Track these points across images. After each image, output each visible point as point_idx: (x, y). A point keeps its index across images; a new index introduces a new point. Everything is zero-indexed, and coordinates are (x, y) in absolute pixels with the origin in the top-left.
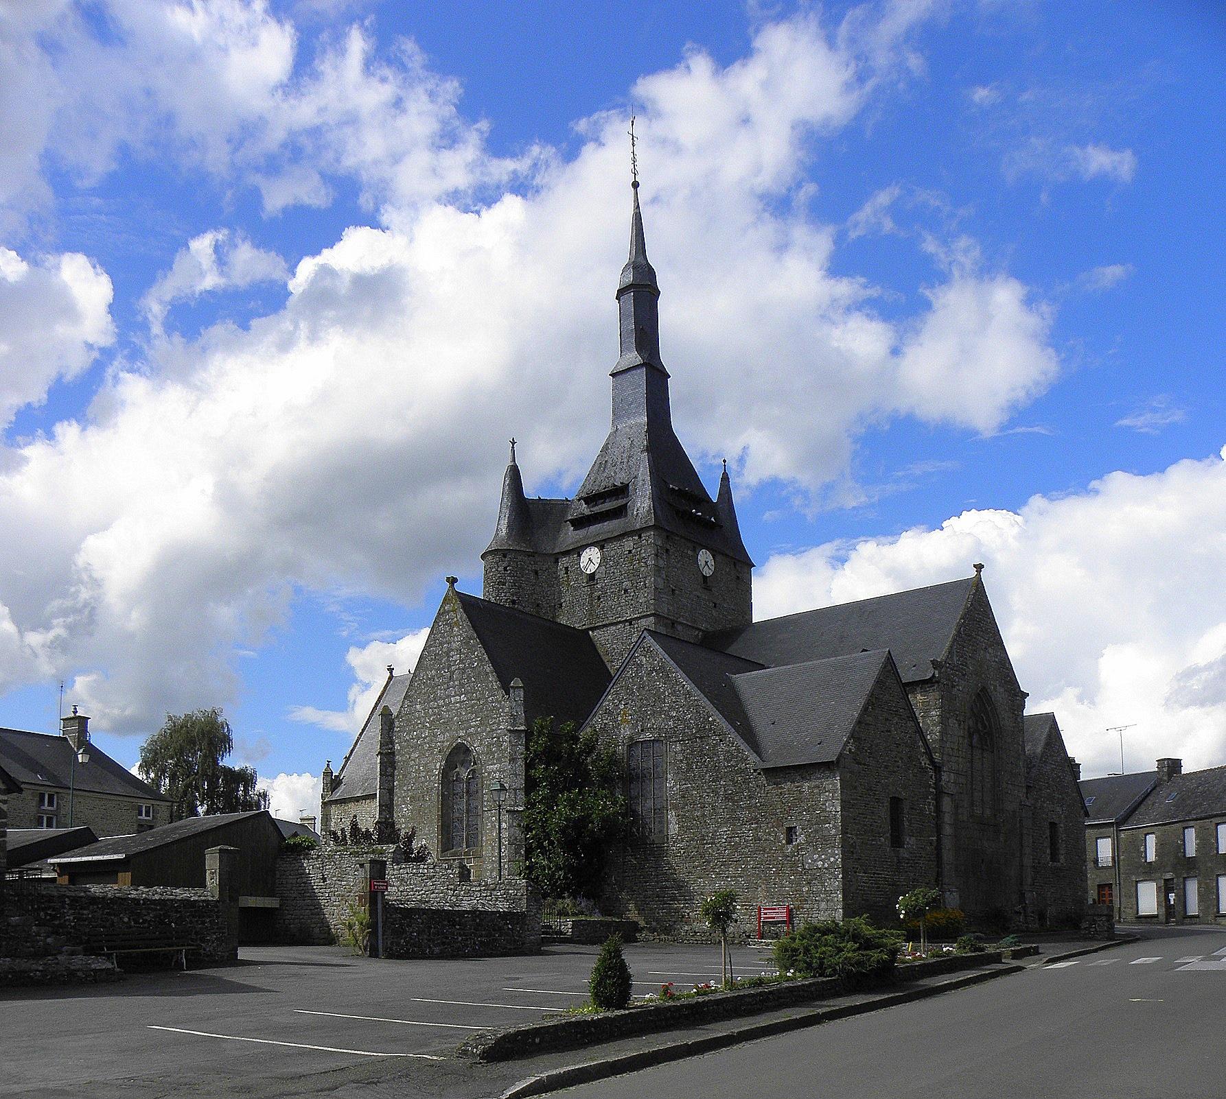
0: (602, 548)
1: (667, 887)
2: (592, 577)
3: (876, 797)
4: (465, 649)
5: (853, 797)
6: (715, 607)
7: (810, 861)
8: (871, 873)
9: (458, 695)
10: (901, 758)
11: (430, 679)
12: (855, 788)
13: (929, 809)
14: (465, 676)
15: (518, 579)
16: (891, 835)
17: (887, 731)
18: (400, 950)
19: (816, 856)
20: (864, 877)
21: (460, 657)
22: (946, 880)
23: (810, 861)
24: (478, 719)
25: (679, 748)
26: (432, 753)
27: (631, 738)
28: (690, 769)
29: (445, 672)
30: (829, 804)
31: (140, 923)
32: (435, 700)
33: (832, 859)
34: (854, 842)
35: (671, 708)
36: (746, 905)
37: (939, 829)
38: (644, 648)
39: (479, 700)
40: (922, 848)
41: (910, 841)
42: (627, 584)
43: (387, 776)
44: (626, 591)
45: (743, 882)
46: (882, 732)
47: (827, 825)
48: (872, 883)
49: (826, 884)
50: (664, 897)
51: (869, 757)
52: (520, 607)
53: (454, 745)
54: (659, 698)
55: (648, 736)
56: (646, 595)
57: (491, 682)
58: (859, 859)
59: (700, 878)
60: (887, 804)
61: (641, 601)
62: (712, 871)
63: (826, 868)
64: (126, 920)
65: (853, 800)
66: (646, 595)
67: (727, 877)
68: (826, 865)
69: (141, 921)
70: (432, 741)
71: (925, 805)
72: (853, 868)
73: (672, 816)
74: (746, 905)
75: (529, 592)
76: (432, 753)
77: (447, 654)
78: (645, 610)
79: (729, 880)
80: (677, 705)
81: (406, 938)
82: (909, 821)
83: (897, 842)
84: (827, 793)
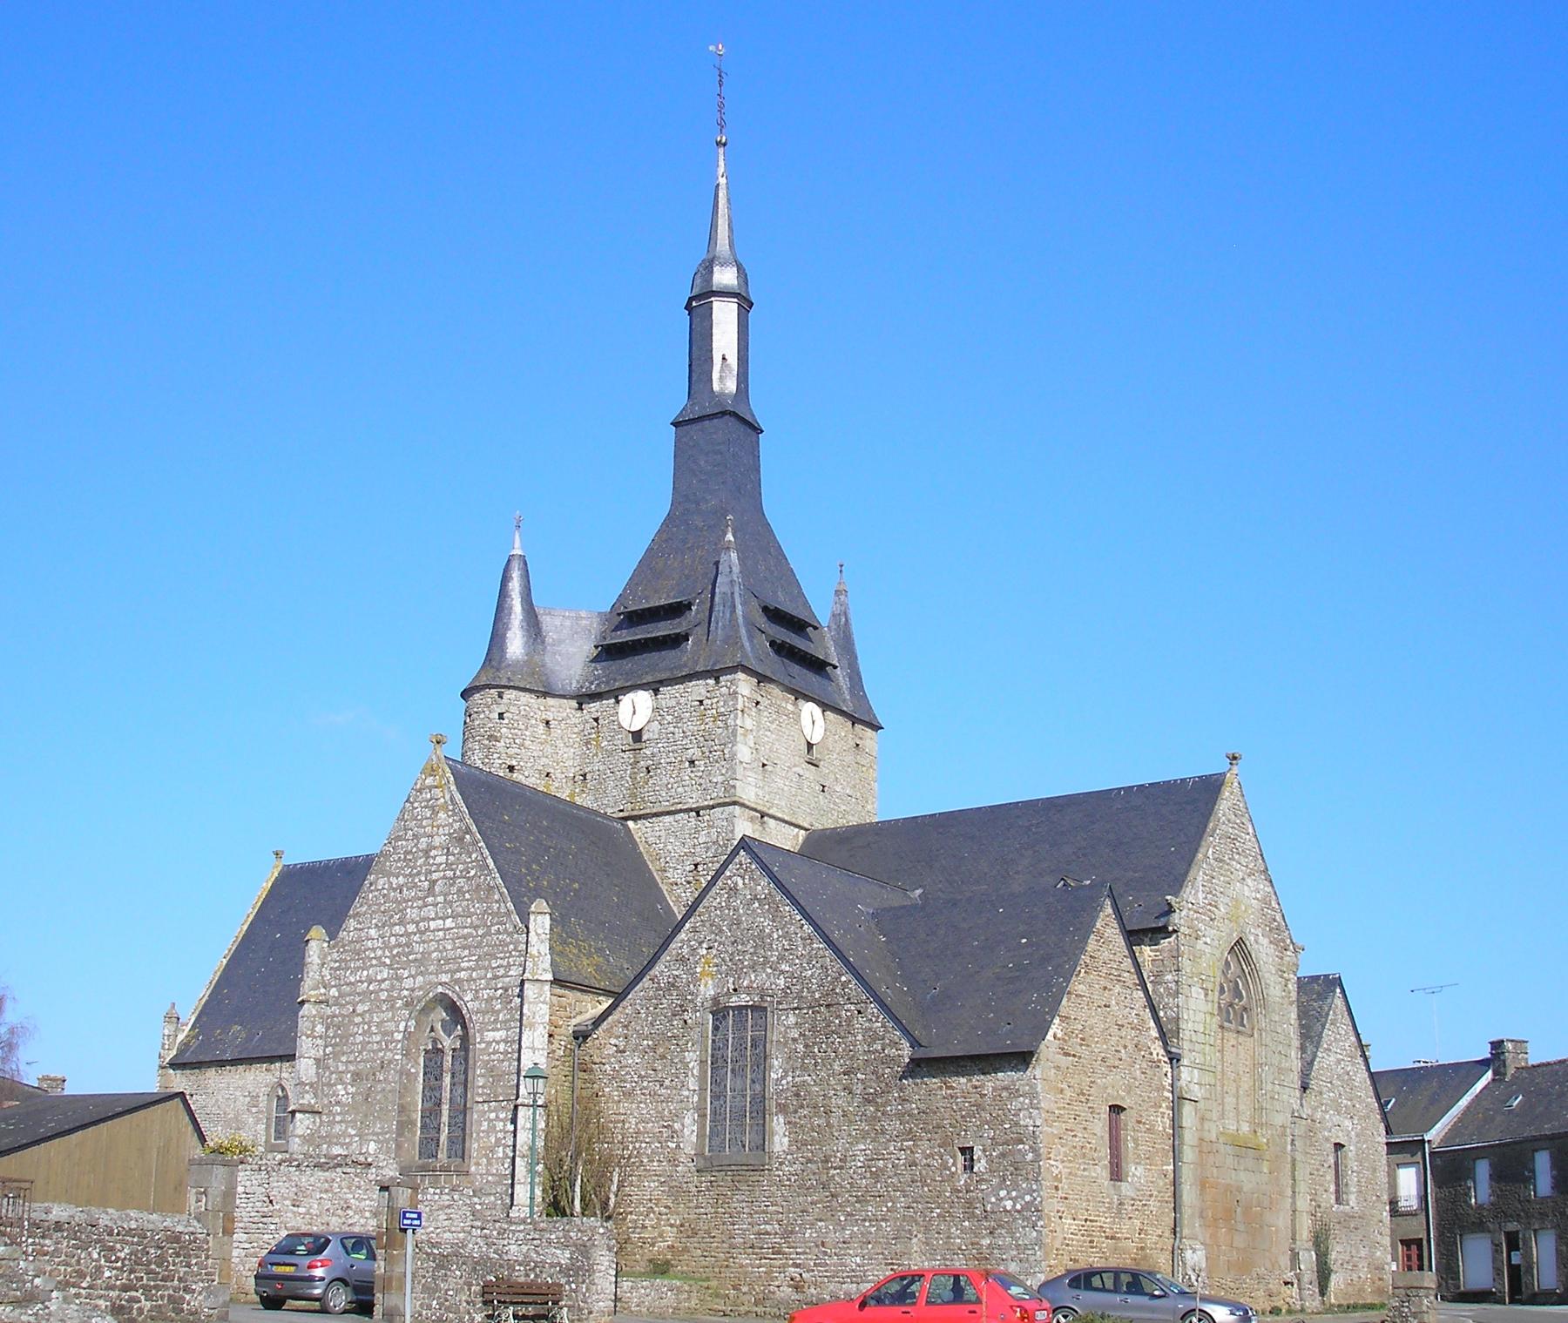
0: (656, 692)
1: (767, 1233)
2: (637, 736)
3: (1089, 1105)
4: (456, 847)
5: (1058, 1105)
6: (823, 791)
7: (993, 1200)
8: (1081, 1220)
9: (441, 918)
10: (1125, 1047)
11: (394, 890)
12: (1062, 1091)
13: (1163, 1123)
14: (454, 890)
15: (519, 733)
16: (1110, 1162)
17: (1105, 1006)
18: (432, 1316)
19: (1003, 1193)
20: (1072, 1225)
21: (447, 859)
22: (1186, 1232)
23: (993, 1200)
24: (474, 958)
25: (792, 1020)
26: (392, 1006)
27: (715, 1000)
28: (808, 1054)
29: (420, 881)
30: (1024, 1116)
31: (111, 1262)
32: (402, 922)
33: (1028, 1198)
34: (1060, 1172)
35: (781, 958)
36: (892, 1264)
37: (1176, 1156)
38: (741, 865)
39: (476, 928)
40: (1152, 1182)
41: (1135, 1172)
42: (694, 752)
43: (316, 1037)
44: (692, 762)
45: (888, 1229)
46: (1099, 1007)
47: (1021, 1146)
48: (1083, 1235)
49: (1018, 1235)
50: (762, 1248)
51: (1081, 1045)
52: (521, 776)
53: (431, 995)
54: (762, 940)
55: (744, 999)
56: (724, 772)
57: (497, 902)
58: (1066, 1198)
59: (821, 1220)
60: (1105, 1116)
61: (715, 780)
62: (839, 1211)
63: (1018, 1212)
64: (95, 1256)
65: (1059, 1108)
66: (724, 772)
67: (865, 1220)
68: (1018, 1207)
69: (113, 1258)
70: (392, 986)
71: (1157, 1116)
72: (1058, 1212)
73: (778, 1124)
74: (892, 1264)
75: (535, 754)
76: (392, 1006)
77: (426, 852)
78: (721, 794)
79: (867, 1224)
80: (791, 954)
81: (439, 1298)
82: (1135, 1140)
83: (1117, 1174)
84: (1021, 1099)
